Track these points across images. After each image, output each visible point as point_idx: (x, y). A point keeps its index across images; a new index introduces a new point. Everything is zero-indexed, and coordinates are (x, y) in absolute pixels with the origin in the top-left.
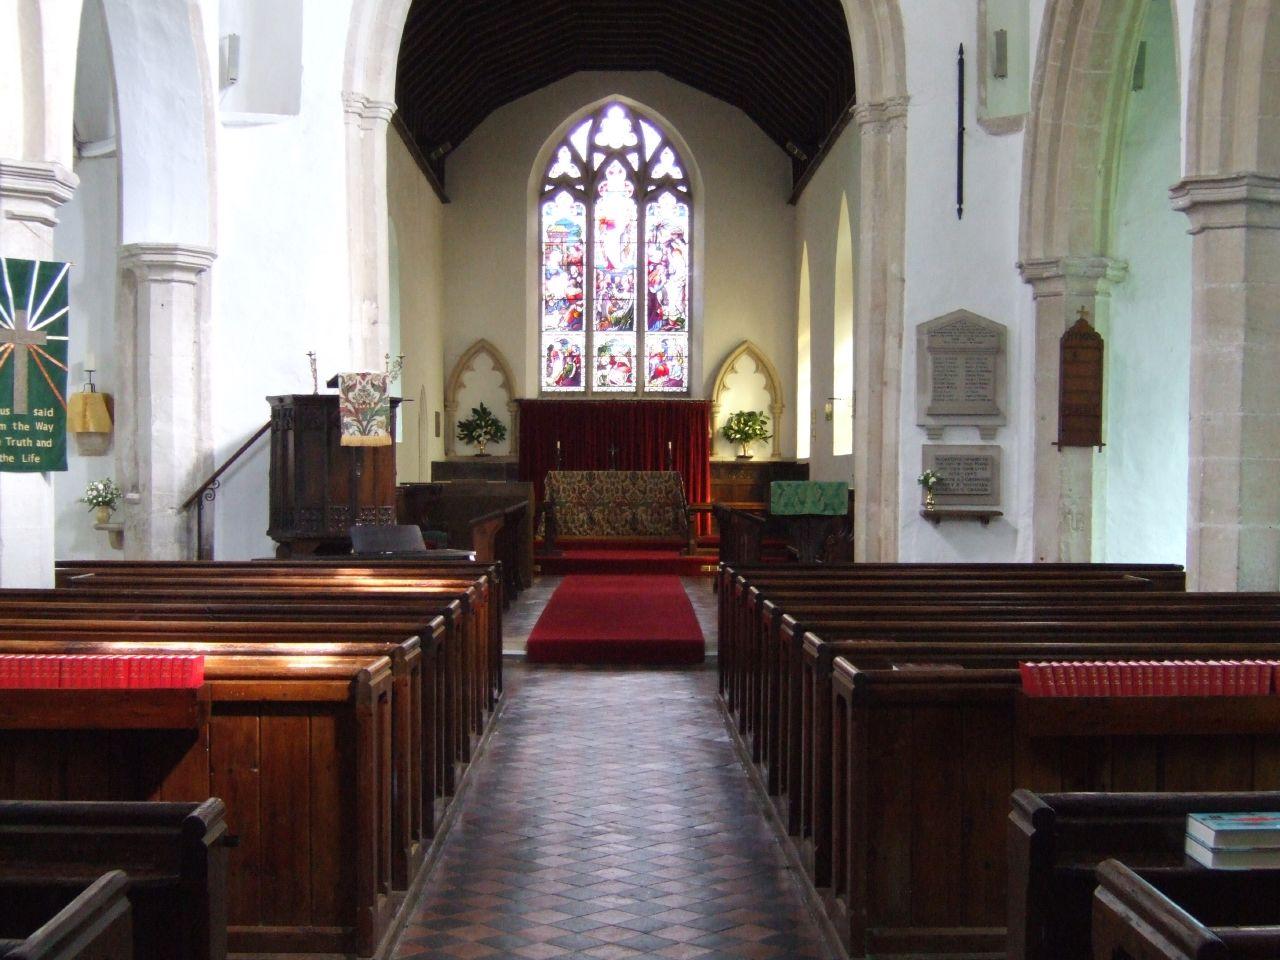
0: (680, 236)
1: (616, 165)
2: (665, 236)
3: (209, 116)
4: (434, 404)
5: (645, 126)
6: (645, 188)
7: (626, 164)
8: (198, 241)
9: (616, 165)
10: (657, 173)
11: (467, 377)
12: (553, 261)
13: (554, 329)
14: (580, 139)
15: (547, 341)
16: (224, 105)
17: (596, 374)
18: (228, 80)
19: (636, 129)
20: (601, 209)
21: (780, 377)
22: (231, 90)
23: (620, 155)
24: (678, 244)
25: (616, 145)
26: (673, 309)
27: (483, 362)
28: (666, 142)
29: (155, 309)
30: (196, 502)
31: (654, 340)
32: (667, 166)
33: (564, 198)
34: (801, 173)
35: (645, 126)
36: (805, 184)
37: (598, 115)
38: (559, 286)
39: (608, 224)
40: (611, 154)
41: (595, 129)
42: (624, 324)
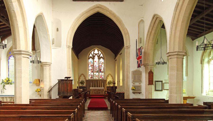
0: (103, 63)
1: (96, 55)
2: (101, 63)
3: (51, 47)
4: (77, 80)
5: (99, 51)
6: (99, 58)
7: (97, 55)
8: (50, 62)
9: (96, 55)
10: (101, 56)
11: (81, 77)
12: (90, 65)
13: (90, 73)
14: (92, 53)
15: (89, 74)
16: (52, 46)
17: (94, 77)
18: (53, 43)
19: (98, 52)
20: (95, 60)
21: (114, 77)
22: (53, 45)
23: (97, 54)
24: (103, 64)
25: (96, 53)
26: (102, 70)
27: (82, 76)
28: (101, 53)
29: (44, 69)
30: (49, 91)
31: (100, 74)
32: (102, 56)
33: (91, 59)
34: (116, 56)
35: (99, 51)
36: (116, 57)
37: (94, 50)
38: (90, 68)
39: (96, 62)
40: (96, 54)
41: (94, 52)
42: (97, 72)
